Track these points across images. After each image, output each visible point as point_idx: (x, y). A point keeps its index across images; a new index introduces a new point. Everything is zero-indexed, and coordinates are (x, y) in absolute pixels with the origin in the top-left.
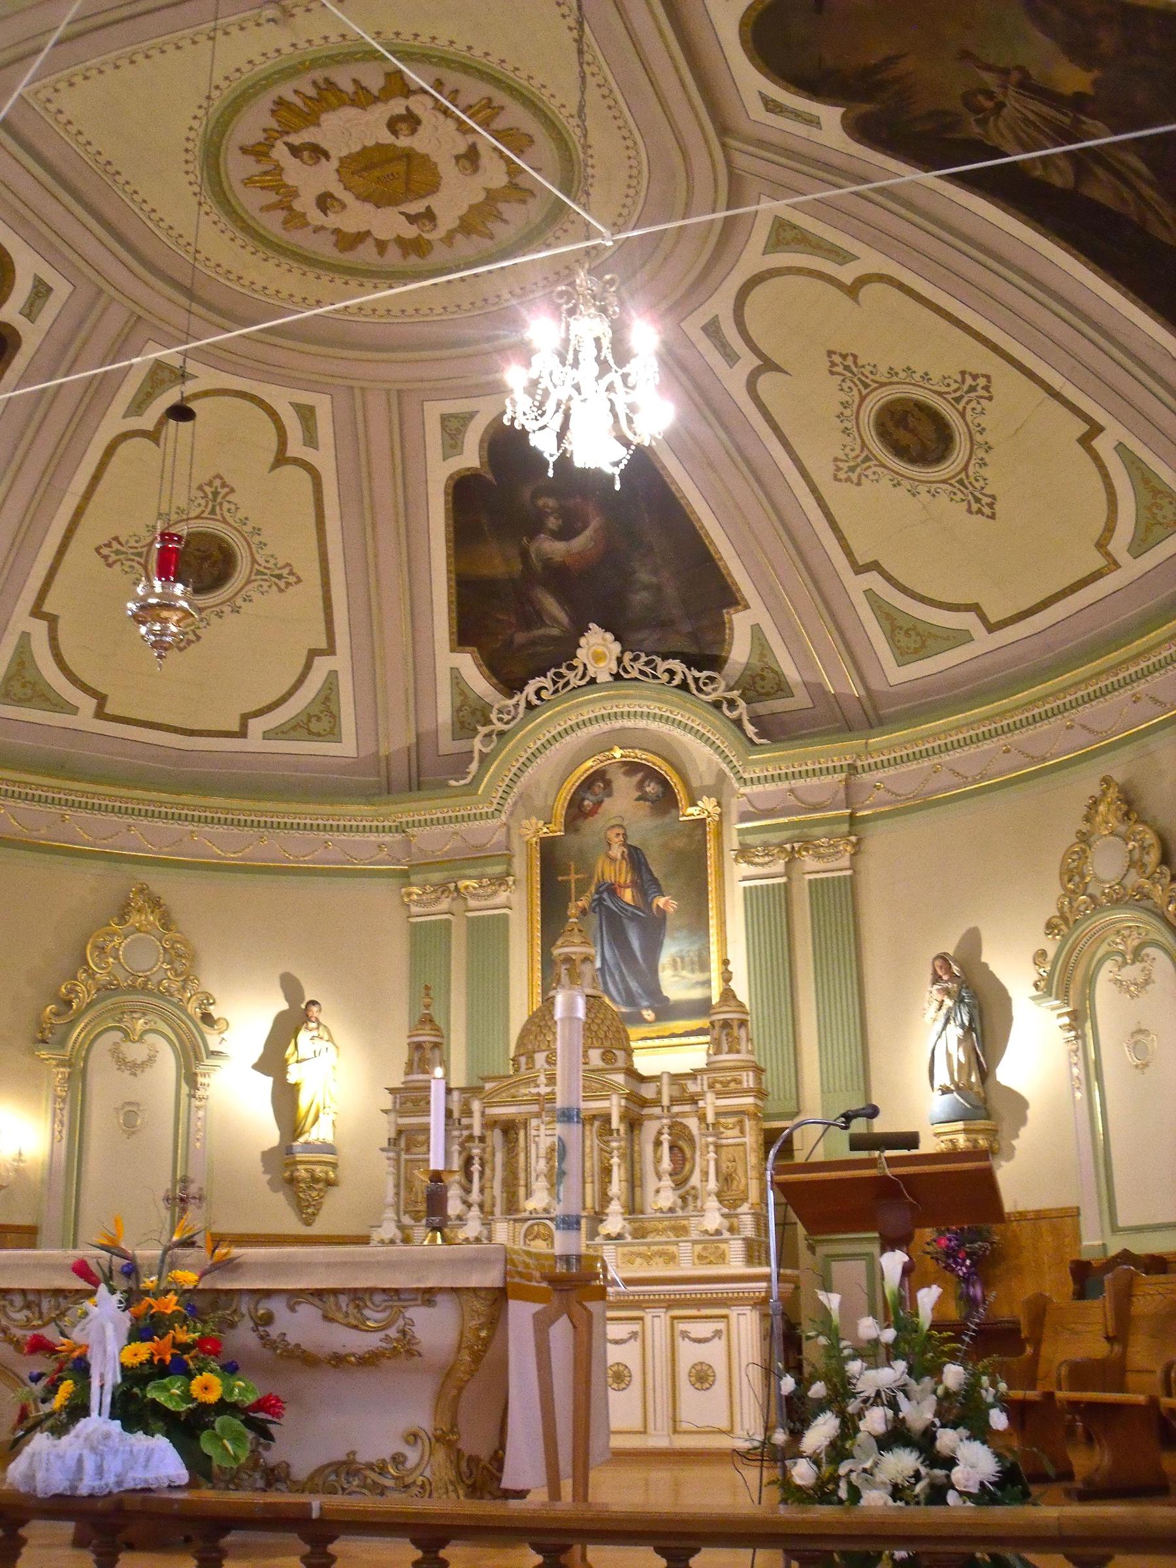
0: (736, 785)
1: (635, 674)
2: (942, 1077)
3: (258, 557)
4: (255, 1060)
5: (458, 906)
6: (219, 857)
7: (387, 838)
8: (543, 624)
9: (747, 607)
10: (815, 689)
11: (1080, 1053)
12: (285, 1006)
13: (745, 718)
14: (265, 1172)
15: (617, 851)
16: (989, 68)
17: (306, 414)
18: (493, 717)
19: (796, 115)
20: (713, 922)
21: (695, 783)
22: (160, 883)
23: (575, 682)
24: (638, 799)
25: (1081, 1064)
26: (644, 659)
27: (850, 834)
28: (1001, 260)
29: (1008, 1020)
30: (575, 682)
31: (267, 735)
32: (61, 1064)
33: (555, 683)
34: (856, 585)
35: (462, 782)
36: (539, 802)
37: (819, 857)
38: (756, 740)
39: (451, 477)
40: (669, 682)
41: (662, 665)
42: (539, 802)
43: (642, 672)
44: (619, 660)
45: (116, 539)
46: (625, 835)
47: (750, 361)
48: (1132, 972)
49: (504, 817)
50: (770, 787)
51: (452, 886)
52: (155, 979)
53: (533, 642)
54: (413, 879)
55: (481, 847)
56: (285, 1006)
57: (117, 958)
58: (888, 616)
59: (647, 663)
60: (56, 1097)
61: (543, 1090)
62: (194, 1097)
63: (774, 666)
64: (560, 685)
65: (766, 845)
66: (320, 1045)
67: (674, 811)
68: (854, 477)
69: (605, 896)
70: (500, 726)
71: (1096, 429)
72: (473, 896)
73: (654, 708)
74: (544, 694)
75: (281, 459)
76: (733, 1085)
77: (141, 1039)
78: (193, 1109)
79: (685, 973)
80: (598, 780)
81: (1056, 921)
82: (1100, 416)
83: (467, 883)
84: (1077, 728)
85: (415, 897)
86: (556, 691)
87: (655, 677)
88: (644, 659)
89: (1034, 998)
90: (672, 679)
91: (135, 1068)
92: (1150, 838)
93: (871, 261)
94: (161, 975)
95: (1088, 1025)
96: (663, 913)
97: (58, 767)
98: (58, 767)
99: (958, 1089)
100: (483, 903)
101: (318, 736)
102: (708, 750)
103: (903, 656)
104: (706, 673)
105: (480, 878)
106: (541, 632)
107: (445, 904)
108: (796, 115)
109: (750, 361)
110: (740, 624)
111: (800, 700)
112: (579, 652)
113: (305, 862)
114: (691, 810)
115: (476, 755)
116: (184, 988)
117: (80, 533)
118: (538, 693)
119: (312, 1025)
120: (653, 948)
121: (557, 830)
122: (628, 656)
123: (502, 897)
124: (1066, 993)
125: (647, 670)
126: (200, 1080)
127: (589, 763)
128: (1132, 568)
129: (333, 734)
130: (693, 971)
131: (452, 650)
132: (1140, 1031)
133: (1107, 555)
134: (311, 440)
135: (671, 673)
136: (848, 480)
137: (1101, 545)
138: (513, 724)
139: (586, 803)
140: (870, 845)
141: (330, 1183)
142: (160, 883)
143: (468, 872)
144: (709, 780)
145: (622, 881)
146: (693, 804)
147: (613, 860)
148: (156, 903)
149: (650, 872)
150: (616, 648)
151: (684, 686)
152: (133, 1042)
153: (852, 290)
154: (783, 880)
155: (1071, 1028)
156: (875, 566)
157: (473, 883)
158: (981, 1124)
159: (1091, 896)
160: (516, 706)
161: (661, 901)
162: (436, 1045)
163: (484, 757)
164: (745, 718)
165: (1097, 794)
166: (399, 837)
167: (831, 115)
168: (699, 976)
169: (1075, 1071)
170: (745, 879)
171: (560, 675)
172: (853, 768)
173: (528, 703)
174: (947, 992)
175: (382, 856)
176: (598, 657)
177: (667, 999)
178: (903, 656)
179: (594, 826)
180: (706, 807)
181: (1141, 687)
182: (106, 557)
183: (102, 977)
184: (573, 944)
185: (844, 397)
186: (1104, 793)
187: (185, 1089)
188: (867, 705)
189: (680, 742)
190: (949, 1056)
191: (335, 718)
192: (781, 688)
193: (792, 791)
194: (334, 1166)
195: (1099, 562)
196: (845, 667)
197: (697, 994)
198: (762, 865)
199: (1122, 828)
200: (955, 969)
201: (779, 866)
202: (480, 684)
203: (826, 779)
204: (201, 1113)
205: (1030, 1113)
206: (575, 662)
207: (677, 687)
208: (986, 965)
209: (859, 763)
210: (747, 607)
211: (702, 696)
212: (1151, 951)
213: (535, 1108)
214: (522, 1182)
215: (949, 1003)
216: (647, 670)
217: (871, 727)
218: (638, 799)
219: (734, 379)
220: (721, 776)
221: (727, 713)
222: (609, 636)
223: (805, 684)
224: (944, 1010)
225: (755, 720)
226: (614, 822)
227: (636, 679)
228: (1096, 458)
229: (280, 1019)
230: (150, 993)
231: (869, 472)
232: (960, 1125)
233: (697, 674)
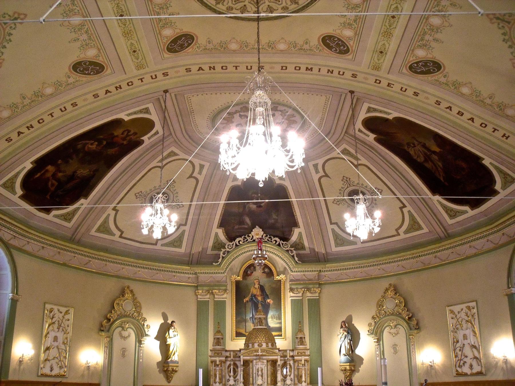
0: (290, 272)
1: (266, 240)
2: (343, 351)
3: (174, 199)
4: (155, 336)
5: (212, 296)
6: (146, 278)
7: (191, 276)
8: (244, 225)
9: (299, 227)
10: (313, 250)
11: (379, 348)
12: (163, 321)
13: (295, 255)
14: (158, 368)
15: (257, 286)
16: (417, 141)
17: (202, 167)
18: (226, 247)
19: (365, 134)
20: (282, 307)
21: (278, 270)
22: (134, 286)
23: (249, 240)
24: (263, 273)
25: (379, 351)
26: (269, 236)
27: (319, 287)
28: (396, 169)
29: (359, 338)
30: (249, 240)
31: (162, 245)
32: (107, 337)
33: (244, 240)
34: (330, 227)
35: (217, 264)
36: (235, 270)
37: (311, 293)
38: (298, 262)
39: (232, 186)
40: (275, 243)
41: (273, 239)
42: (235, 270)
43: (268, 240)
44: (262, 236)
45: (141, 192)
46: (259, 282)
47: (322, 173)
48: (393, 331)
49: (226, 274)
50: (299, 273)
51: (211, 291)
52: (132, 313)
53: (241, 228)
54: (199, 288)
55: (218, 281)
56: (163, 321)
57: (122, 307)
58: (336, 235)
59: (269, 238)
60: (105, 347)
61: (260, 354)
62: (140, 347)
63: (302, 242)
64: (246, 240)
65: (297, 288)
66: (175, 333)
67: (272, 277)
68: (338, 203)
69: (253, 298)
70: (228, 250)
72: (217, 295)
73: (272, 250)
74: (241, 242)
75: (191, 176)
76: (303, 354)
77: (126, 330)
78: (140, 350)
79: (274, 320)
80: (252, 267)
81: (375, 316)
83: (215, 291)
84: (381, 270)
85: (200, 293)
86: (244, 242)
87: (271, 242)
88: (269, 236)
89: (368, 335)
90: (276, 243)
91: (125, 338)
92: (402, 300)
93: (363, 161)
94: (133, 312)
95: (381, 342)
96: (269, 304)
97: (106, 250)
98: (106, 250)
99: (348, 355)
100: (220, 297)
101: (175, 247)
102: (282, 262)
103: (337, 245)
104: (285, 242)
105: (219, 290)
106: (243, 226)
107: (208, 296)
108: (365, 134)
109: (322, 173)
110: (296, 232)
111: (307, 251)
112: (252, 233)
113: (168, 281)
114: (277, 277)
115: (221, 257)
116: (139, 316)
117: (133, 189)
118: (239, 242)
119: (173, 328)
120: (266, 313)
121: (239, 278)
122: (265, 235)
123: (225, 296)
124: (377, 334)
125: (270, 239)
126: (142, 342)
127: (250, 262)
128: (402, 236)
129: (180, 246)
130: (277, 320)
131: (217, 228)
132: (395, 345)
133: (398, 232)
134: (200, 173)
135: (276, 241)
136: (336, 203)
138: (231, 249)
139: (248, 272)
140: (323, 291)
141: (176, 371)
142: (134, 286)
143: (215, 288)
144: (282, 269)
145: (258, 294)
146: (278, 276)
147: (256, 288)
148: (132, 291)
149: (266, 292)
150: (262, 233)
151: (279, 245)
152: (124, 330)
154: (301, 298)
155: (377, 342)
156: (336, 224)
157: (217, 291)
158: (353, 364)
159: (385, 312)
160: (233, 244)
161: (269, 301)
162: (222, 338)
163: (223, 258)
164: (295, 255)
165: (388, 288)
166: (194, 276)
167: (372, 136)
168: (278, 321)
169: (377, 353)
170: (291, 297)
171: (246, 238)
172: (320, 271)
173: (236, 244)
174: (345, 331)
175: (190, 280)
176: (257, 234)
177: (270, 326)
178: (337, 245)
179: (251, 279)
180: (282, 277)
181: (400, 263)
182: (137, 196)
183: (118, 313)
184: (261, 315)
185: (343, 186)
186: (390, 287)
187: (137, 344)
188: (325, 256)
189: (274, 259)
190: (345, 347)
191: (181, 242)
192: (303, 248)
193: (304, 275)
194: (177, 366)
195: (395, 233)
196: (322, 245)
197: (278, 326)
198: (296, 294)
199: (395, 297)
200: (347, 325)
201: (300, 295)
202: (222, 237)
203: (314, 273)
204: (142, 352)
205: (364, 361)
206: (250, 235)
207: (277, 245)
208: (354, 325)
209: (322, 270)
210: (299, 227)
211: (284, 248)
212: (399, 326)
213: (255, 357)
214: (251, 376)
215: (346, 333)
216: (270, 239)
217: (325, 262)
218: (263, 273)
219: (316, 177)
220: (285, 268)
221: (291, 254)
222: (261, 230)
223: (309, 248)
224: (344, 335)
225: (298, 255)
226: (256, 278)
227: (266, 242)
228: (402, 212)
229: (162, 325)
230: (130, 317)
231: (342, 203)
232: (348, 364)
233: (283, 242)
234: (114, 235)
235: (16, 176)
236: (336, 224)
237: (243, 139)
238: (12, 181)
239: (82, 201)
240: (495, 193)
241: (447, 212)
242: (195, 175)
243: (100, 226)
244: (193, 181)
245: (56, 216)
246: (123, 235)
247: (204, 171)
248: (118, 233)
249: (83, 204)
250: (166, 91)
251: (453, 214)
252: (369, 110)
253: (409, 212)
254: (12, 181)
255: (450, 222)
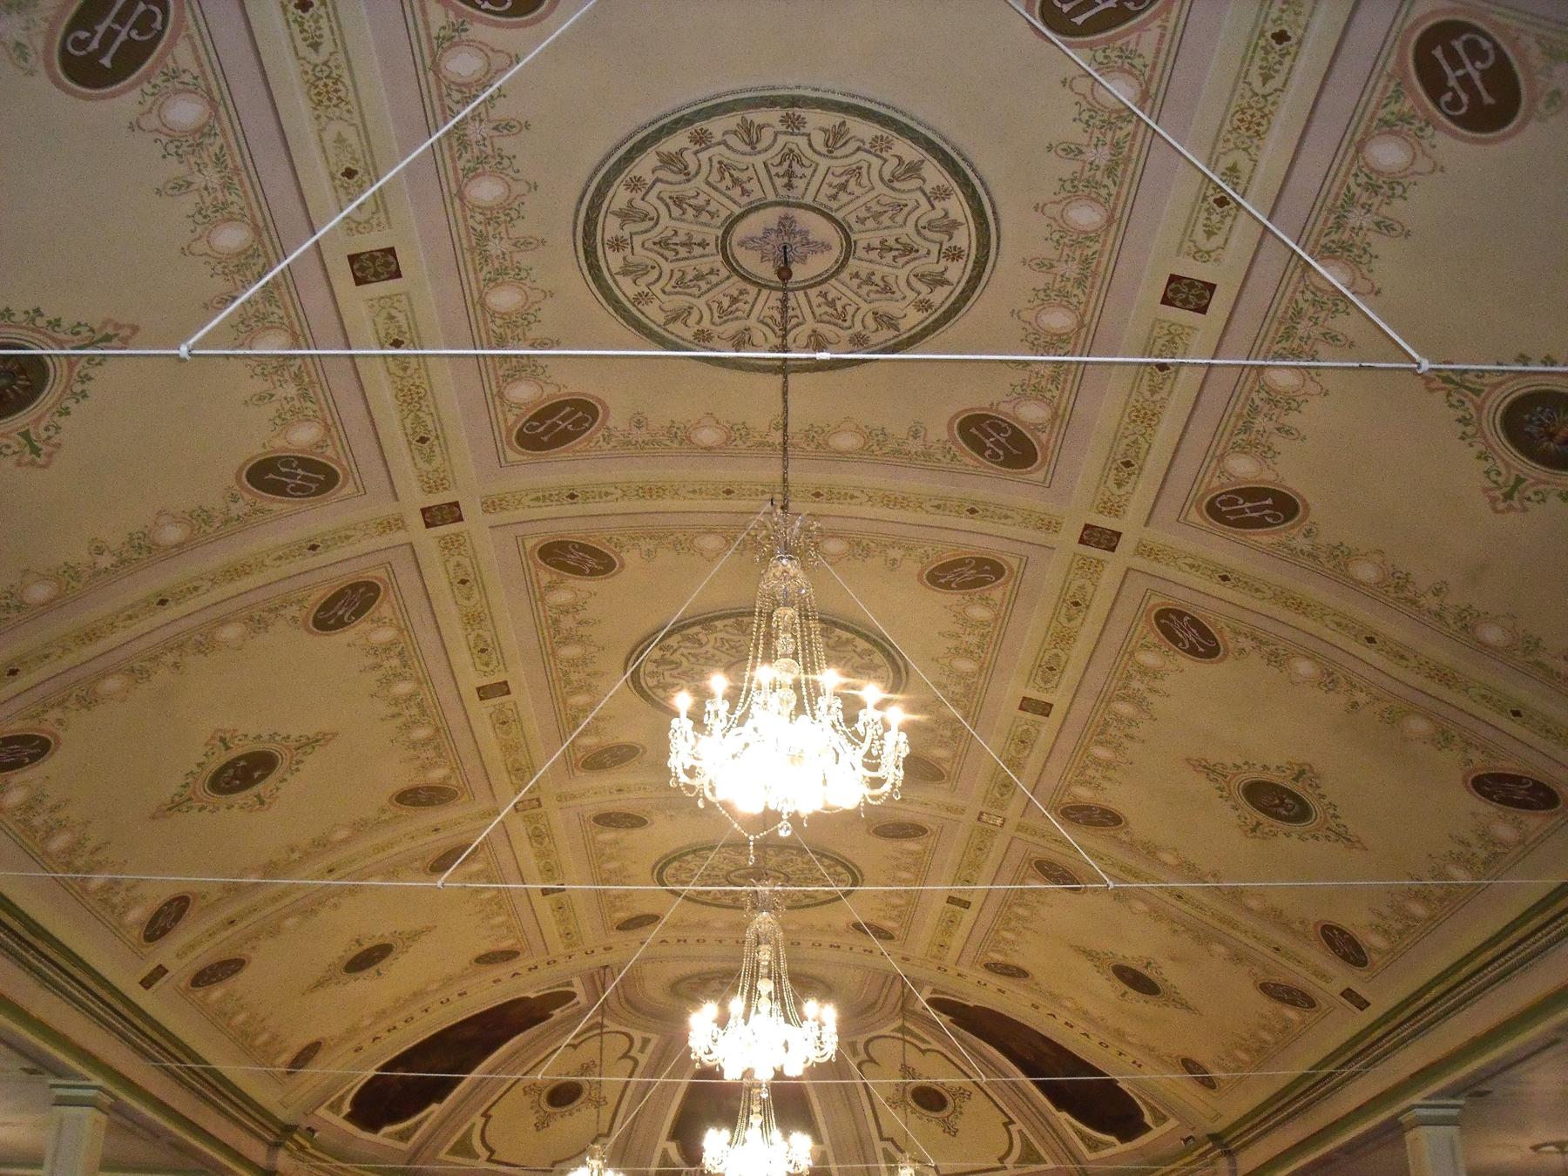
17: (646, 1041)
47: (864, 1056)
71: (1012, 1122)
75: (626, 1056)
82: (1015, 1118)
93: (936, 1045)
134: (642, 1050)
137: (1001, 1160)
153: (924, 1052)
228: (1009, 1131)
234: (477, 1157)
235: (348, 1092)
236: (892, 1140)
237: (723, 1022)
238: (342, 1098)
239: (434, 1107)
240: (1147, 1129)
241: (1082, 1140)
242: (632, 1053)
243: (456, 1143)
244: (630, 1064)
245: (389, 1136)
246: (495, 1157)
247: (650, 1048)
248: (484, 1154)
249: (435, 1109)
250: (605, 967)
251: (1094, 1146)
252: (935, 991)
253: (1020, 1131)
254: (342, 1098)
255: (1091, 1156)
